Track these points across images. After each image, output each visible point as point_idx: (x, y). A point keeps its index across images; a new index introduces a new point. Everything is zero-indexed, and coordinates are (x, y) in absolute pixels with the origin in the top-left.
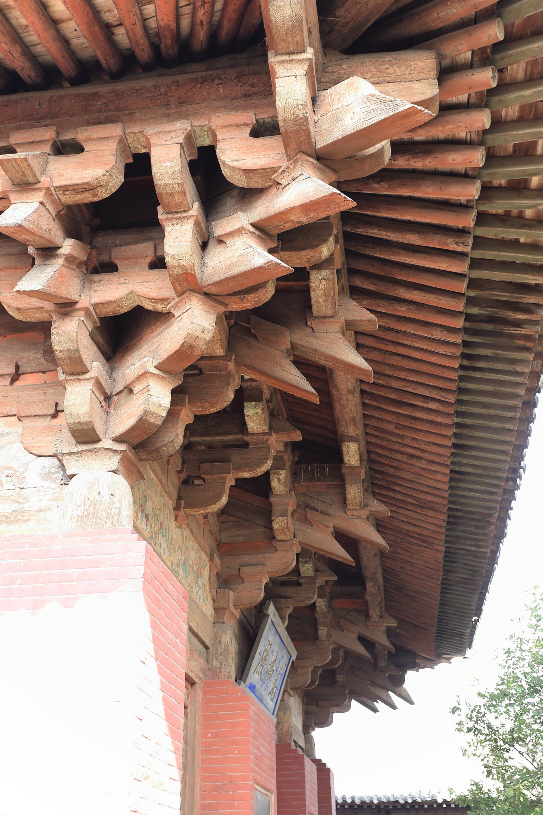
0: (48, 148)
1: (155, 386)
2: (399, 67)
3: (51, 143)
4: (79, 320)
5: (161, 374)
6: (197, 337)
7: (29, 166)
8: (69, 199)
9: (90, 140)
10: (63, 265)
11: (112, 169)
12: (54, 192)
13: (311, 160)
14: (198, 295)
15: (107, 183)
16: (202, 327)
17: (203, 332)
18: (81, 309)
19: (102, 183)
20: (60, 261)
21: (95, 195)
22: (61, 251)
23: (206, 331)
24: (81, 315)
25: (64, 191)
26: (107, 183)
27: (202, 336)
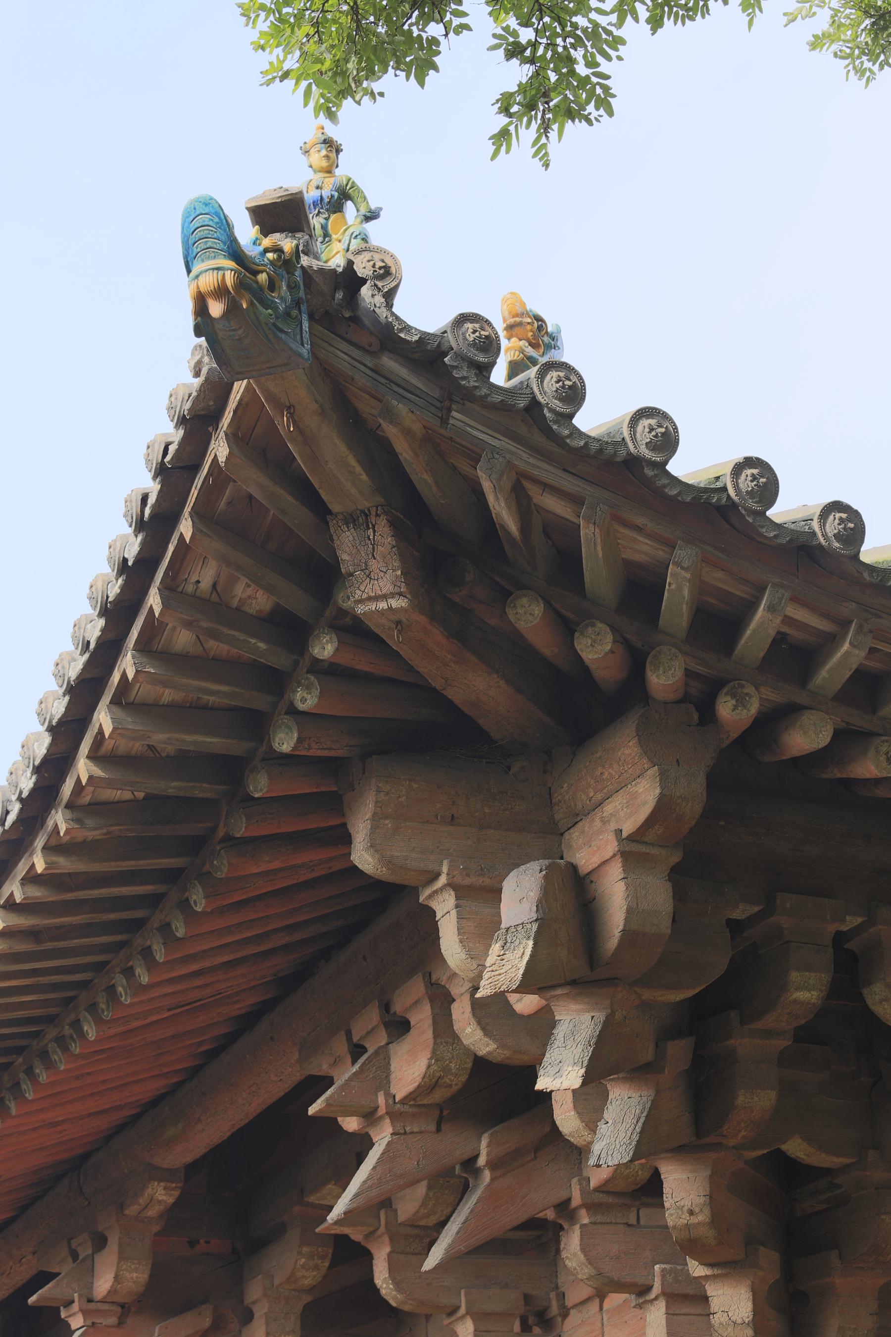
0: (382, 1038)
1: (720, 1292)
2: (611, 766)
3: (382, 1026)
4: (583, 1226)
5: (716, 1271)
6: (687, 1226)
7: (341, 1106)
8: (437, 1097)
9: (409, 1008)
10: (493, 1179)
11: (434, 1052)
12: (406, 1108)
13: (559, 992)
14: (663, 1155)
15: (446, 1070)
16: (686, 1208)
17: (691, 1213)
18: (580, 1207)
19: (438, 1074)
20: (487, 1175)
21: (450, 1086)
22: (482, 1161)
23: (697, 1210)
24: (585, 1218)
25: (414, 1100)
26: (446, 1070)
27: (694, 1220)
